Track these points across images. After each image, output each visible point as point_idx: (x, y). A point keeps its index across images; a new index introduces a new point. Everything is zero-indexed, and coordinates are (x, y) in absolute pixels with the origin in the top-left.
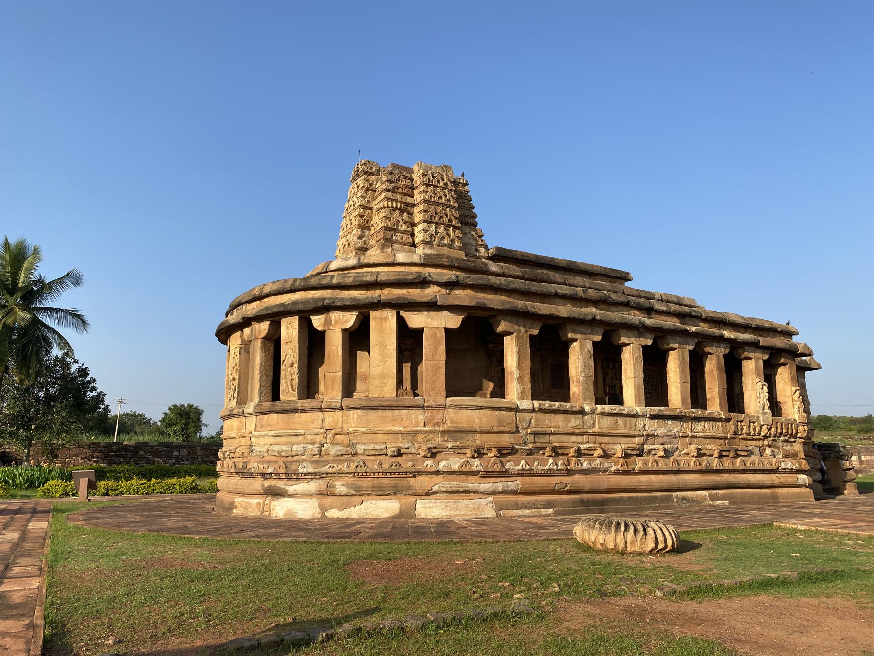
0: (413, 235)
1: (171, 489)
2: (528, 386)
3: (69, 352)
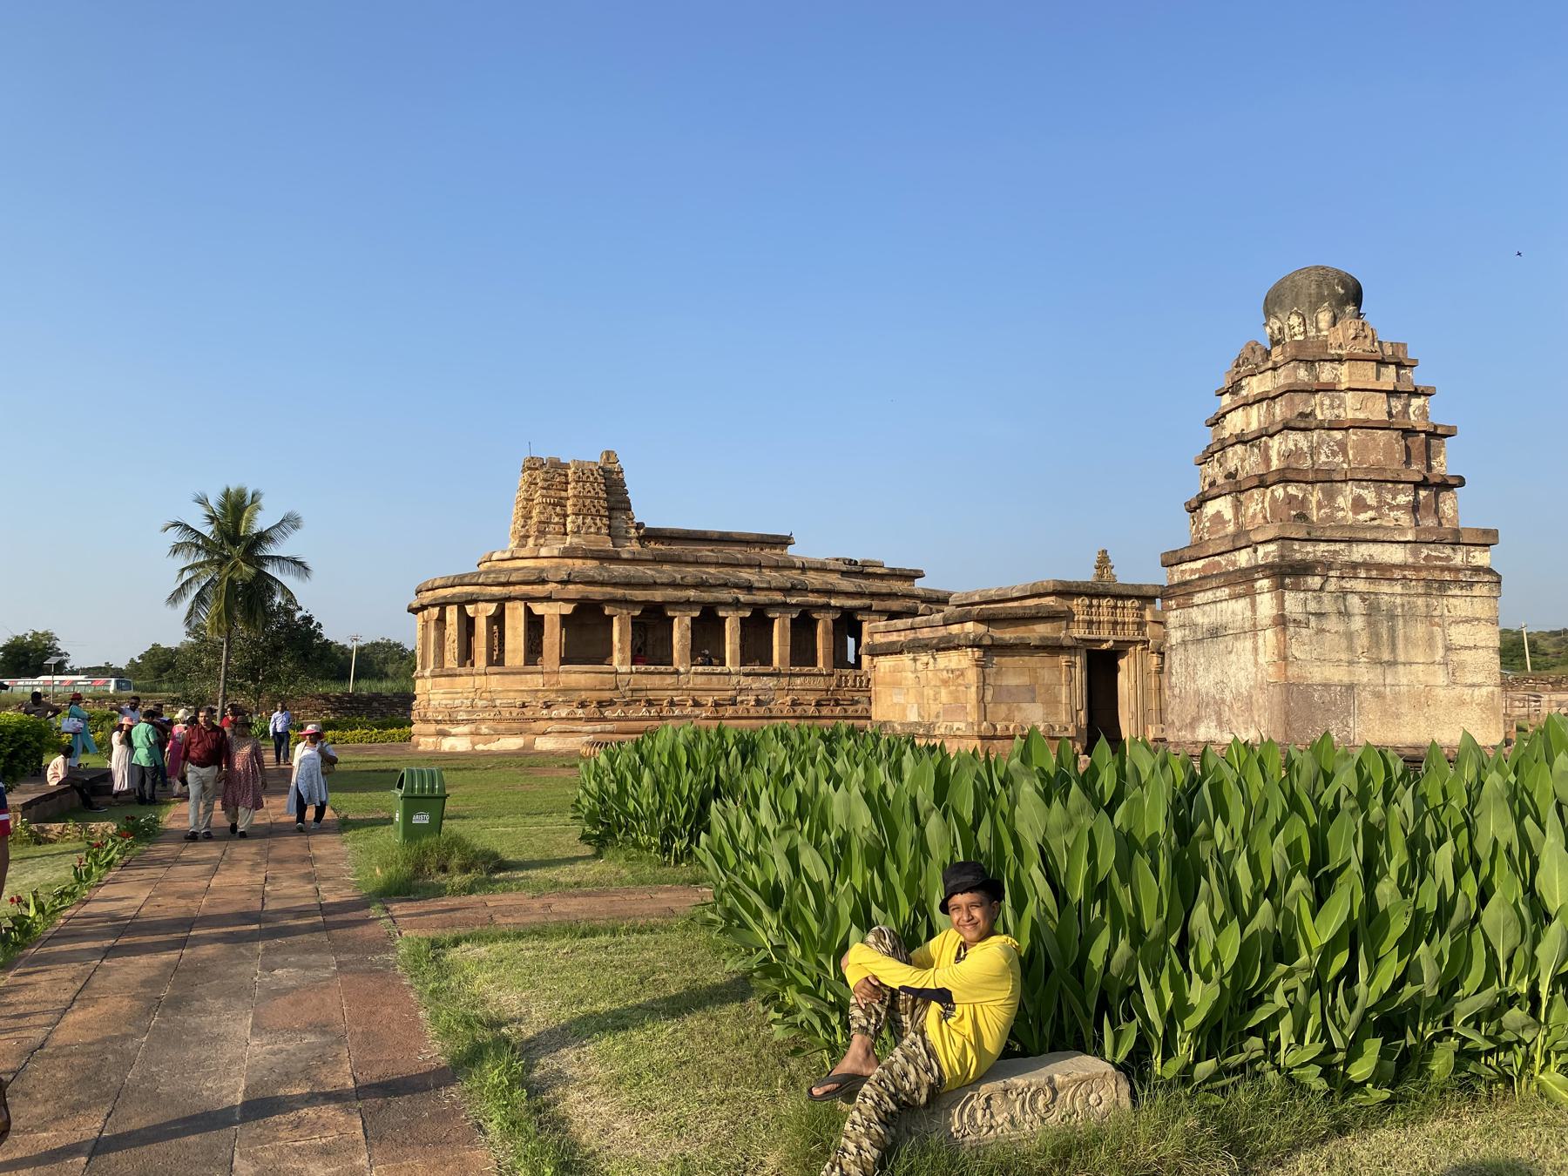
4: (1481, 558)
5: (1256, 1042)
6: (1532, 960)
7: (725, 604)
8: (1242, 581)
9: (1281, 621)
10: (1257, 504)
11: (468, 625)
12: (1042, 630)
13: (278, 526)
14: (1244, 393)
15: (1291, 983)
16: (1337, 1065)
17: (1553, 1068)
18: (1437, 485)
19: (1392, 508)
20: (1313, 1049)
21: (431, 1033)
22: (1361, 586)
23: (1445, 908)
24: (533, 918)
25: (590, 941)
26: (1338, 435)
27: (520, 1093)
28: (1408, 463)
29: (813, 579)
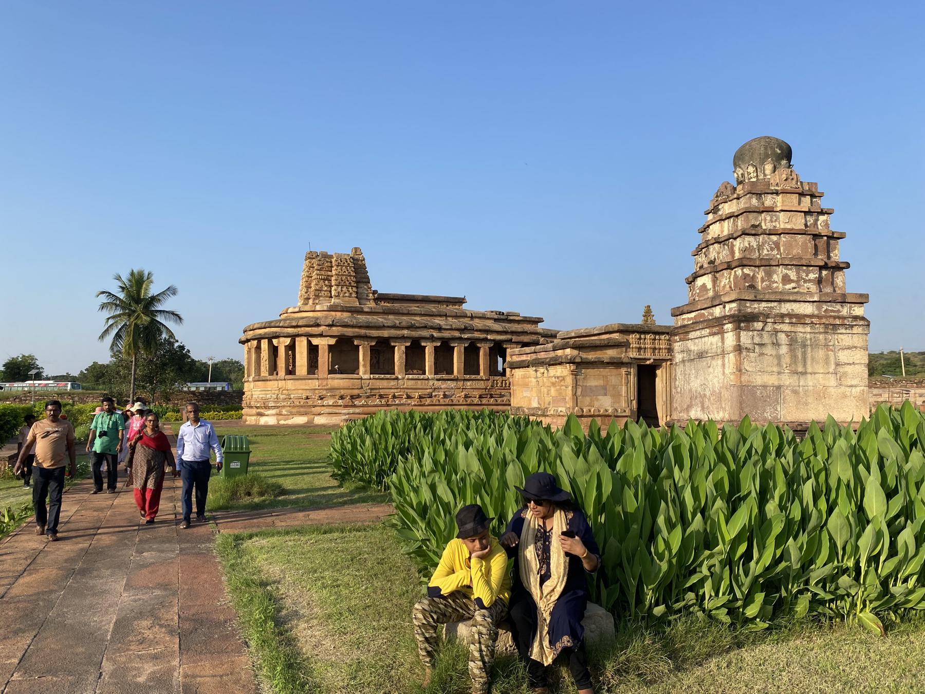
1: (231, 417)
2: (369, 368)
3: (172, 335)
4: (858, 311)
5: (691, 596)
6: (857, 548)
7: (425, 339)
8: (716, 325)
9: (739, 349)
10: (726, 279)
11: (274, 350)
12: (611, 353)
13: (163, 293)
14: (720, 213)
15: (712, 562)
16: (739, 608)
17: (867, 610)
18: (833, 268)
19: (805, 281)
20: (723, 599)
21: (227, 590)
22: (786, 328)
23: (805, 517)
24: (296, 523)
25: (329, 536)
26: (774, 238)
27: (271, 624)
28: (816, 254)
29: (478, 324)
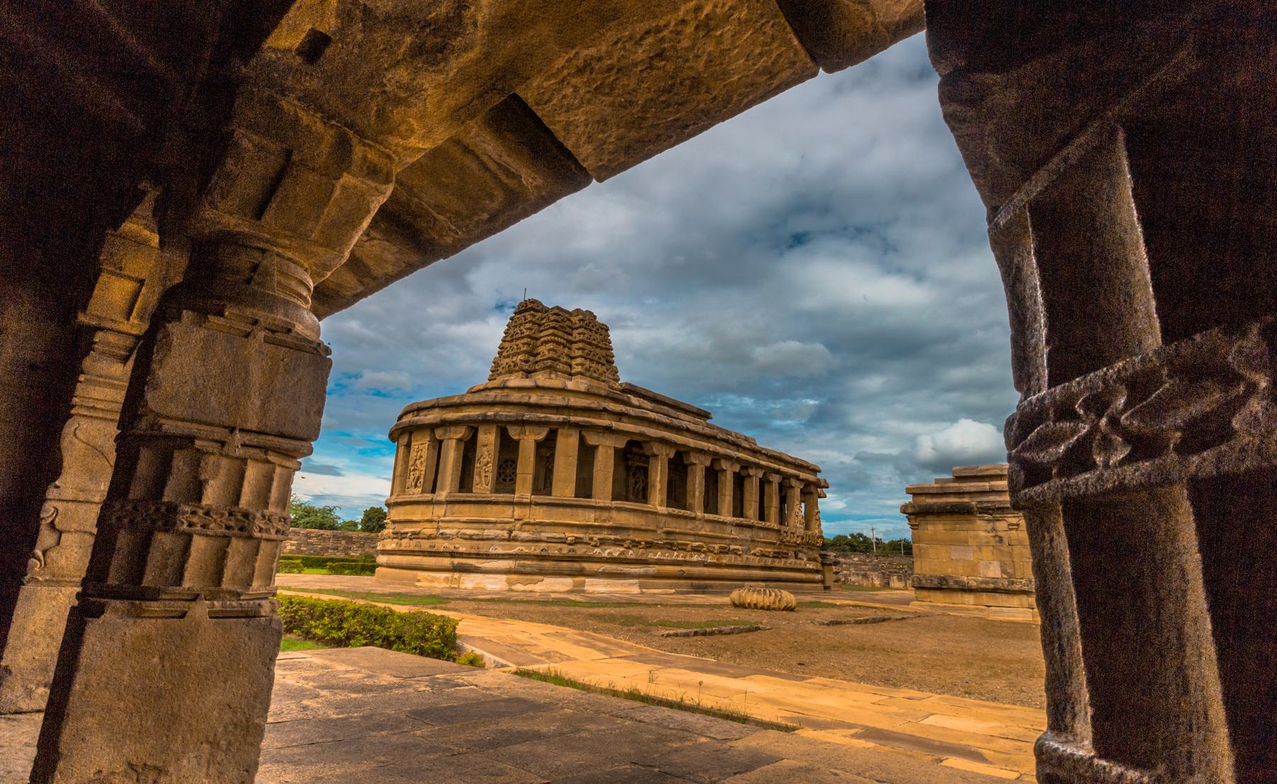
0: (570, 366)
7: (728, 458)
